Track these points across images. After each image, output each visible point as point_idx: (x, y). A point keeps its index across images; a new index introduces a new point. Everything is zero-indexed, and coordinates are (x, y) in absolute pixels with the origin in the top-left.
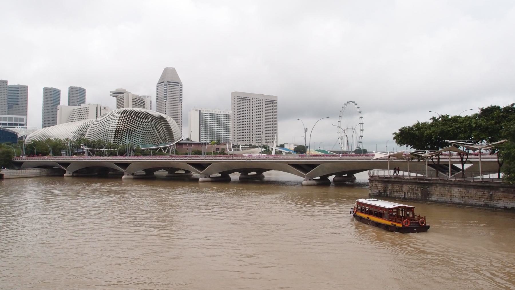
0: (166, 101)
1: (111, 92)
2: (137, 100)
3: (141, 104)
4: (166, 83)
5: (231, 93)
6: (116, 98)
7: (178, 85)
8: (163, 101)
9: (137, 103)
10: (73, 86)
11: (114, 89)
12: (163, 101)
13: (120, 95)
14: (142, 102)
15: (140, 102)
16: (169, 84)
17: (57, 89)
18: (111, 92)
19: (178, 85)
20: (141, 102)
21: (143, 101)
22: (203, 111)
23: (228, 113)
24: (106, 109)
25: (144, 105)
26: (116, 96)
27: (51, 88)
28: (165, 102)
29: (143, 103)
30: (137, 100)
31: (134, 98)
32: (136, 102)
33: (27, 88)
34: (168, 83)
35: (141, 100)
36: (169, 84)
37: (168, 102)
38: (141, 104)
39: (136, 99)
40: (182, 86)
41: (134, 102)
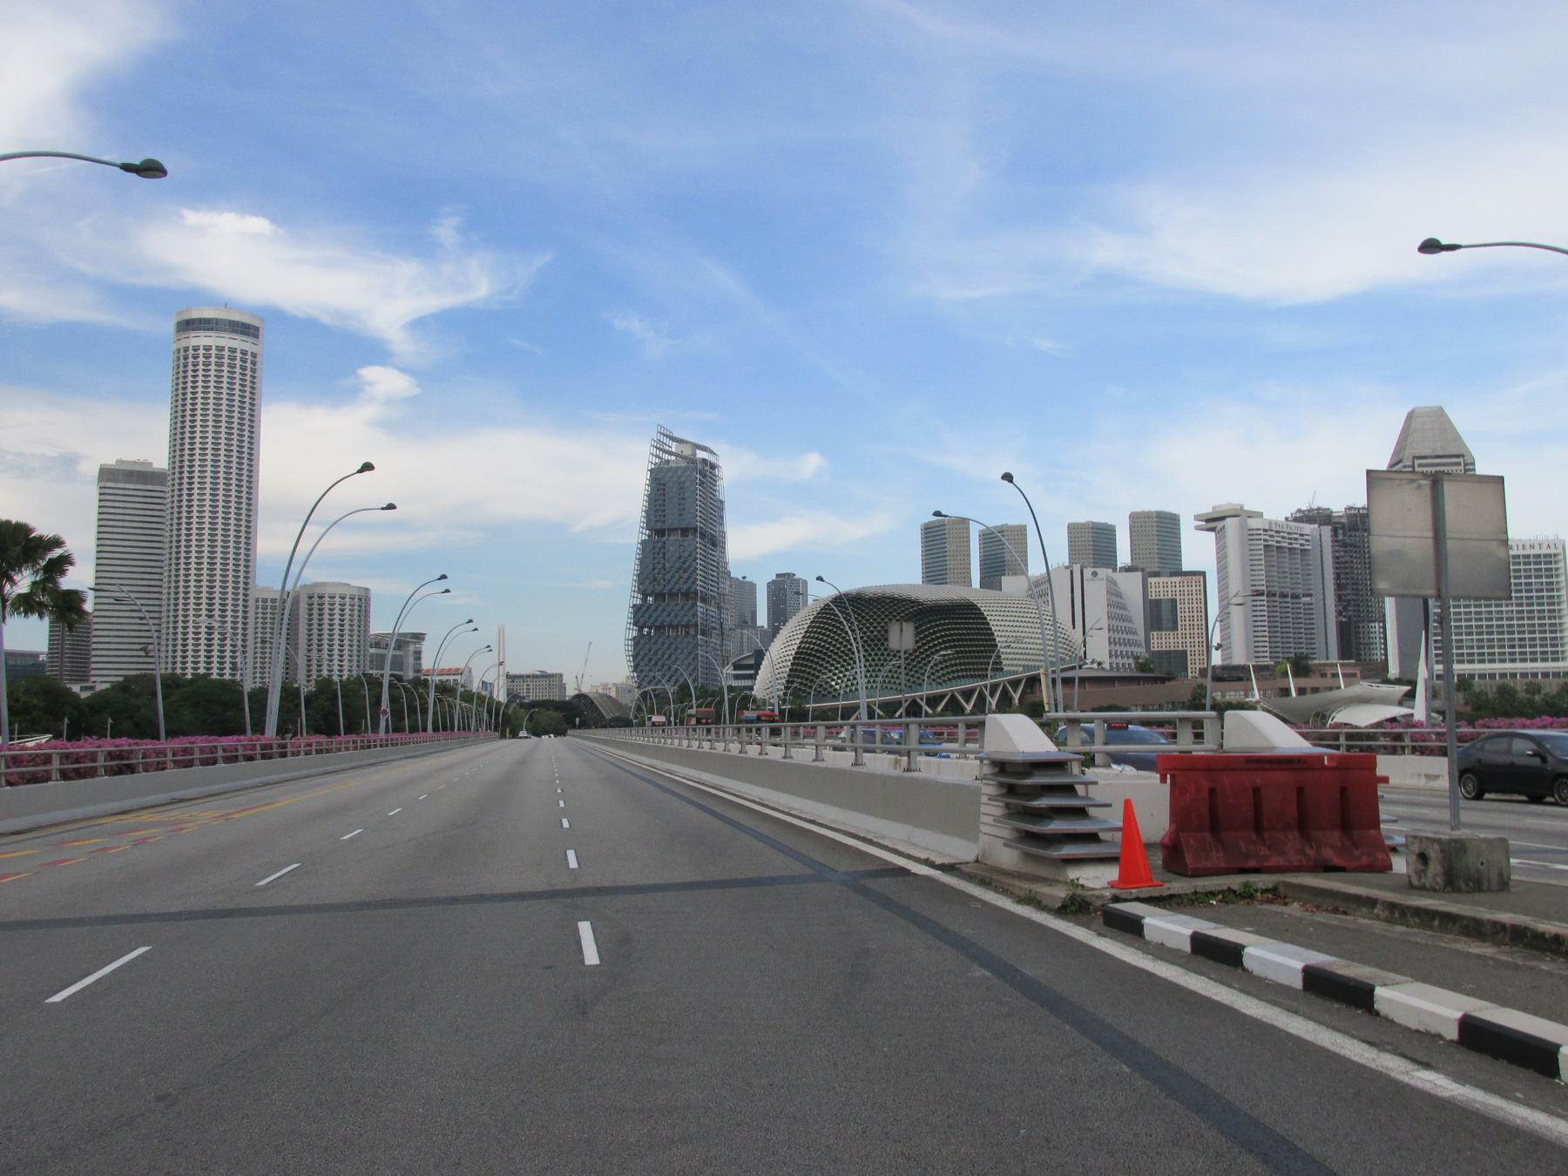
2: (1270, 533)
4: (1409, 463)
5: (1503, 478)
6: (1213, 534)
7: (1459, 464)
10: (1139, 509)
11: (1207, 509)
13: (1219, 525)
14: (1296, 539)
15: (1283, 538)
16: (1420, 465)
17: (1106, 524)
18: (1197, 518)
19: (1459, 464)
20: (1290, 539)
21: (1301, 535)
23: (1544, 546)
24: (1099, 576)
27: (1088, 523)
30: (1270, 533)
32: (1265, 540)
33: (1025, 530)
34: (1417, 462)
35: (1289, 533)
36: (1420, 465)
39: (1265, 530)
40: (1473, 464)
41: (1262, 542)
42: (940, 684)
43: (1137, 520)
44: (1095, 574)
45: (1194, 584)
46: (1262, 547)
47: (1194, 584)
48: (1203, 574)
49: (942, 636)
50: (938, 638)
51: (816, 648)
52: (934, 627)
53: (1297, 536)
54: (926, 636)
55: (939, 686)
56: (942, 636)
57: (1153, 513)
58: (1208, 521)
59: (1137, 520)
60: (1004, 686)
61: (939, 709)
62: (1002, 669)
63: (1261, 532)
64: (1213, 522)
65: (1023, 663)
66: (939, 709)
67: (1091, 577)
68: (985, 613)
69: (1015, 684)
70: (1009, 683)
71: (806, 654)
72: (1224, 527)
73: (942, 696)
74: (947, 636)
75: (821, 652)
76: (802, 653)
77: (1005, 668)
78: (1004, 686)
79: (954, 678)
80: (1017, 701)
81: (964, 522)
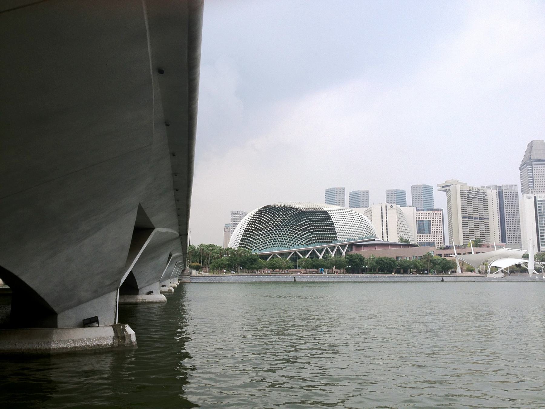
0: (532, 189)
1: (439, 186)
2: (470, 192)
3: (478, 196)
8: (528, 190)
9: (471, 196)
11: (443, 183)
12: (528, 190)
13: (448, 188)
15: (475, 194)
18: (439, 186)
22: (540, 197)
24: (393, 208)
25: (486, 198)
26: (445, 191)
28: (531, 191)
29: (483, 196)
30: (470, 192)
31: (466, 190)
34: (533, 163)
35: (478, 192)
36: (535, 165)
37: (535, 190)
38: (478, 196)
42: (307, 245)
43: (415, 188)
44: (392, 207)
45: (438, 214)
46: (466, 198)
47: (438, 214)
48: (442, 210)
49: (309, 224)
50: (307, 225)
51: (253, 229)
52: (308, 219)
53: (482, 193)
54: (302, 224)
55: (307, 246)
56: (309, 224)
57: (421, 185)
58: (443, 187)
59: (415, 188)
60: (338, 247)
61: (307, 257)
62: (337, 240)
63: (466, 191)
64: (445, 188)
65: (347, 237)
66: (307, 257)
67: (390, 208)
68: (330, 215)
69: (343, 246)
70: (341, 246)
71: (248, 231)
72: (450, 189)
73: (309, 251)
74: (312, 224)
75: (255, 230)
76: (246, 231)
77: (339, 239)
78: (338, 247)
79: (316, 242)
80: (344, 254)
81: (343, 189)
